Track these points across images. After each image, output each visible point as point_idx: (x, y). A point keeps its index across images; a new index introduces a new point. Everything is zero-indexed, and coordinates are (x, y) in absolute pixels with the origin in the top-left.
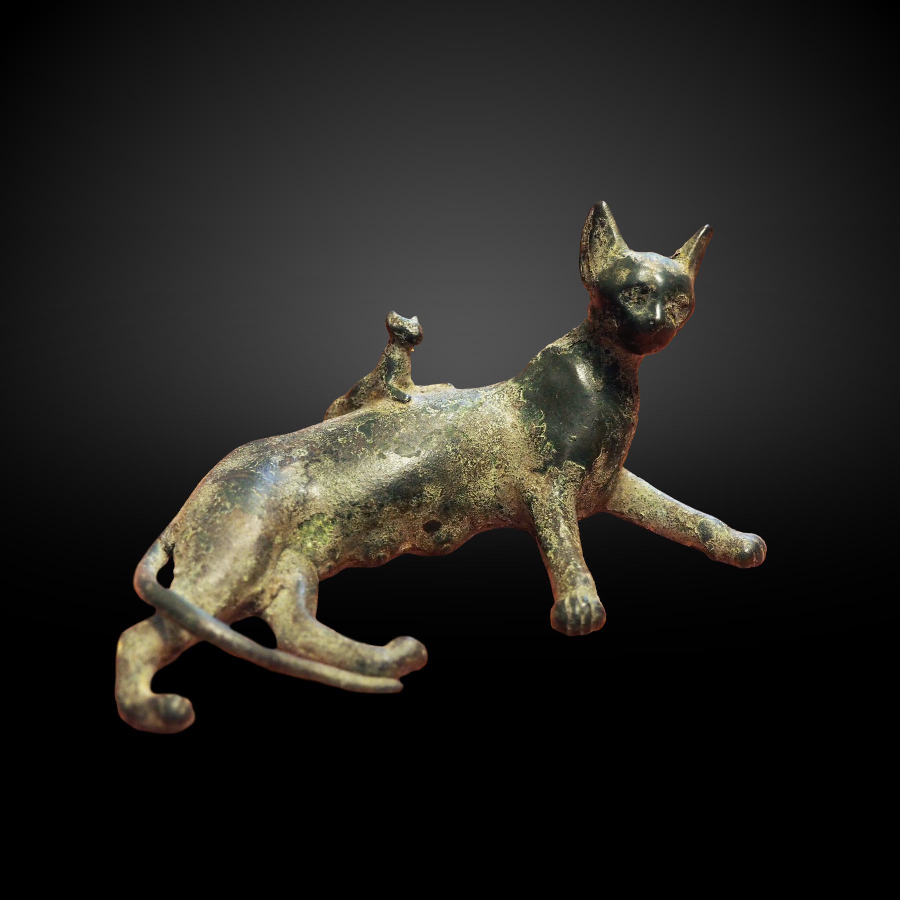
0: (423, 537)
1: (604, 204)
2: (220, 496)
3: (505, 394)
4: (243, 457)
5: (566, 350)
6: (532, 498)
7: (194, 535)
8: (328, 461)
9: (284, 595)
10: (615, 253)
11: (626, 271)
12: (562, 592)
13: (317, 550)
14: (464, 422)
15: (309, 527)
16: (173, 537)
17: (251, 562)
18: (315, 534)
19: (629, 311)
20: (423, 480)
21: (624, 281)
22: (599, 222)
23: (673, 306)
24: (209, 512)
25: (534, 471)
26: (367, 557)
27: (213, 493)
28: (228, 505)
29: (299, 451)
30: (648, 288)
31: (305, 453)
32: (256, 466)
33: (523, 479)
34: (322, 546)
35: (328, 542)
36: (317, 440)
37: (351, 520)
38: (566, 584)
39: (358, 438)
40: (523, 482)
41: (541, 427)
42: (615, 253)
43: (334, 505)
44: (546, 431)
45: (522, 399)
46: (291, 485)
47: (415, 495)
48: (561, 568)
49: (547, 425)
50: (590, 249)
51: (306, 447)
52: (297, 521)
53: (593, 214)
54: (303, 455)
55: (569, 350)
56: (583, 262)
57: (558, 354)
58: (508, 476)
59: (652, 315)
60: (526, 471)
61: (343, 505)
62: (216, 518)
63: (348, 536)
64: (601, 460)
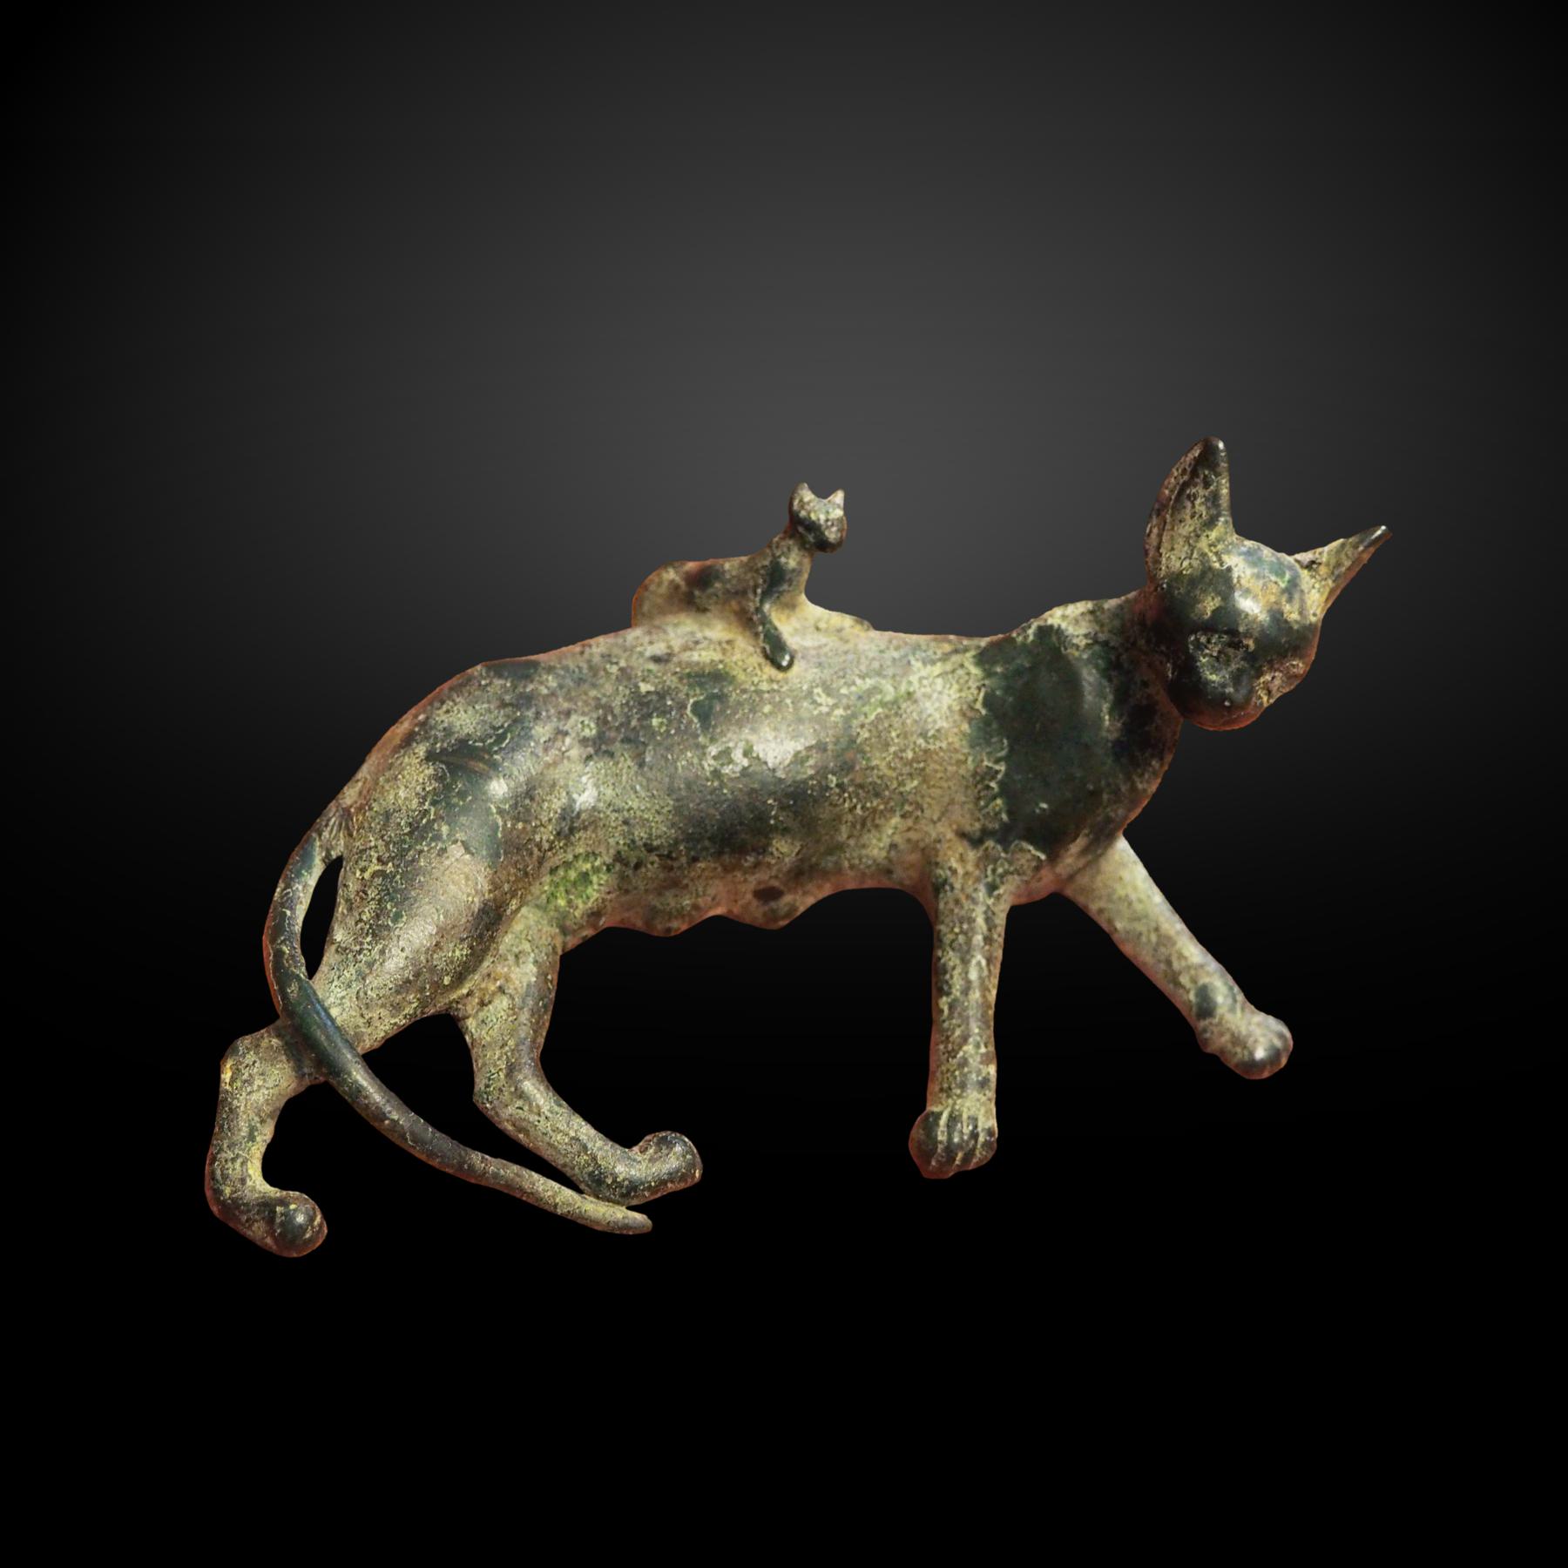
0: (749, 903)
1: (1221, 445)
2: (434, 803)
3: (954, 683)
4: (485, 706)
5: (1077, 647)
6: (945, 882)
7: (375, 874)
8: (625, 760)
9: (502, 1003)
10: (1210, 546)
11: (1216, 600)
12: (942, 1090)
13: (572, 911)
14: (870, 731)
15: (567, 871)
16: (342, 842)
17: (460, 953)
18: (574, 884)
19: (1197, 667)
20: (774, 829)
21: (1206, 617)
22: (1202, 476)
23: (1273, 678)
24: (410, 834)
25: (962, 835)
26: (648, 923)
27: (424, 789)
28: (445, 829)
29: (582, 722)
30: (1241, 642)
31: (591, 730)
32: (504, 745)
33: (939, 841)
34: (581, 906)
35: (592, 900)
36: (617, 703)
37: (639, 871)
38: (951, 1079)
39: (686, 727)
40: (938, 846)
41: (997, 767)
42: (1210, 546)
43: (618, 843)
44: (1003, 777)
45: (978, 706)
46: (556, 797)
47: (754, 850)
48: (953, 1043)
49: (1006, 770)
50: (1173, 508)
51: (595, 715)
52: (551, 864)
53: (1197, 455)
54: (587, 733)
55: (1084, 650)
56: (1154, 517)
57: (1062, 649)
58: (916, 830)
59: (1231, 690)
60: (949, 830)
61: (632, 846)
62: (421, 852)
63: (627, 892)
64: (1075, 847)
